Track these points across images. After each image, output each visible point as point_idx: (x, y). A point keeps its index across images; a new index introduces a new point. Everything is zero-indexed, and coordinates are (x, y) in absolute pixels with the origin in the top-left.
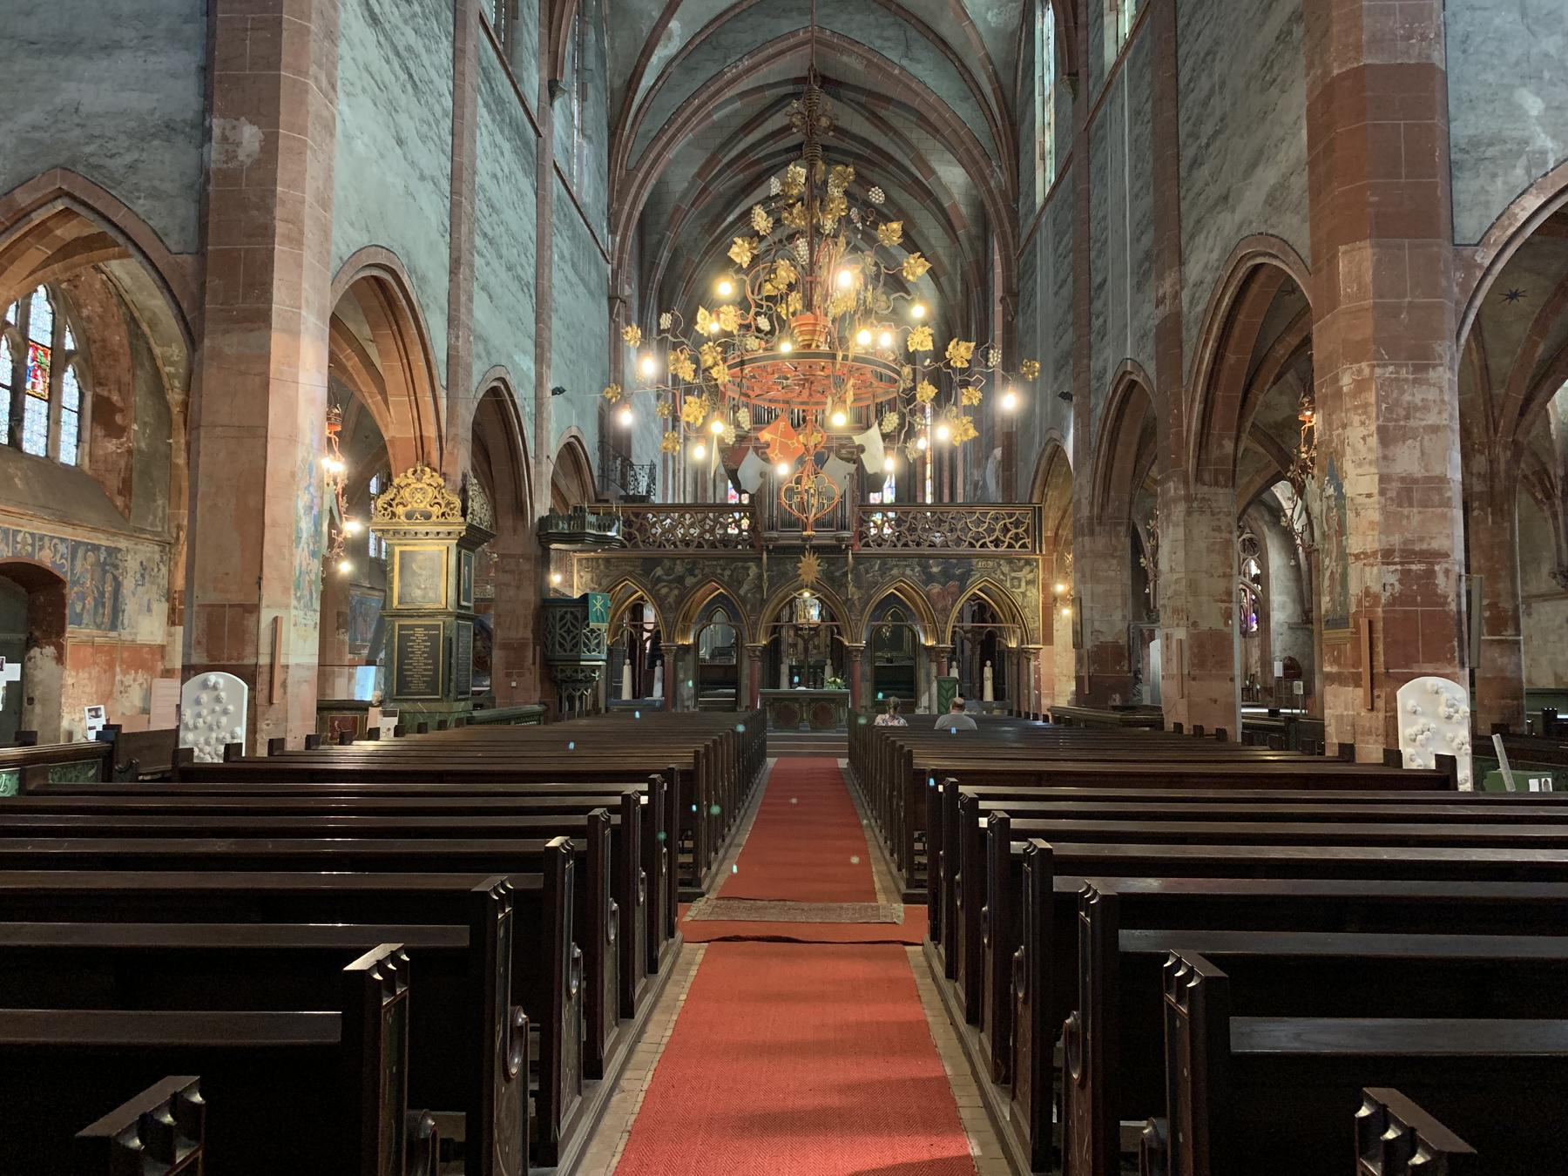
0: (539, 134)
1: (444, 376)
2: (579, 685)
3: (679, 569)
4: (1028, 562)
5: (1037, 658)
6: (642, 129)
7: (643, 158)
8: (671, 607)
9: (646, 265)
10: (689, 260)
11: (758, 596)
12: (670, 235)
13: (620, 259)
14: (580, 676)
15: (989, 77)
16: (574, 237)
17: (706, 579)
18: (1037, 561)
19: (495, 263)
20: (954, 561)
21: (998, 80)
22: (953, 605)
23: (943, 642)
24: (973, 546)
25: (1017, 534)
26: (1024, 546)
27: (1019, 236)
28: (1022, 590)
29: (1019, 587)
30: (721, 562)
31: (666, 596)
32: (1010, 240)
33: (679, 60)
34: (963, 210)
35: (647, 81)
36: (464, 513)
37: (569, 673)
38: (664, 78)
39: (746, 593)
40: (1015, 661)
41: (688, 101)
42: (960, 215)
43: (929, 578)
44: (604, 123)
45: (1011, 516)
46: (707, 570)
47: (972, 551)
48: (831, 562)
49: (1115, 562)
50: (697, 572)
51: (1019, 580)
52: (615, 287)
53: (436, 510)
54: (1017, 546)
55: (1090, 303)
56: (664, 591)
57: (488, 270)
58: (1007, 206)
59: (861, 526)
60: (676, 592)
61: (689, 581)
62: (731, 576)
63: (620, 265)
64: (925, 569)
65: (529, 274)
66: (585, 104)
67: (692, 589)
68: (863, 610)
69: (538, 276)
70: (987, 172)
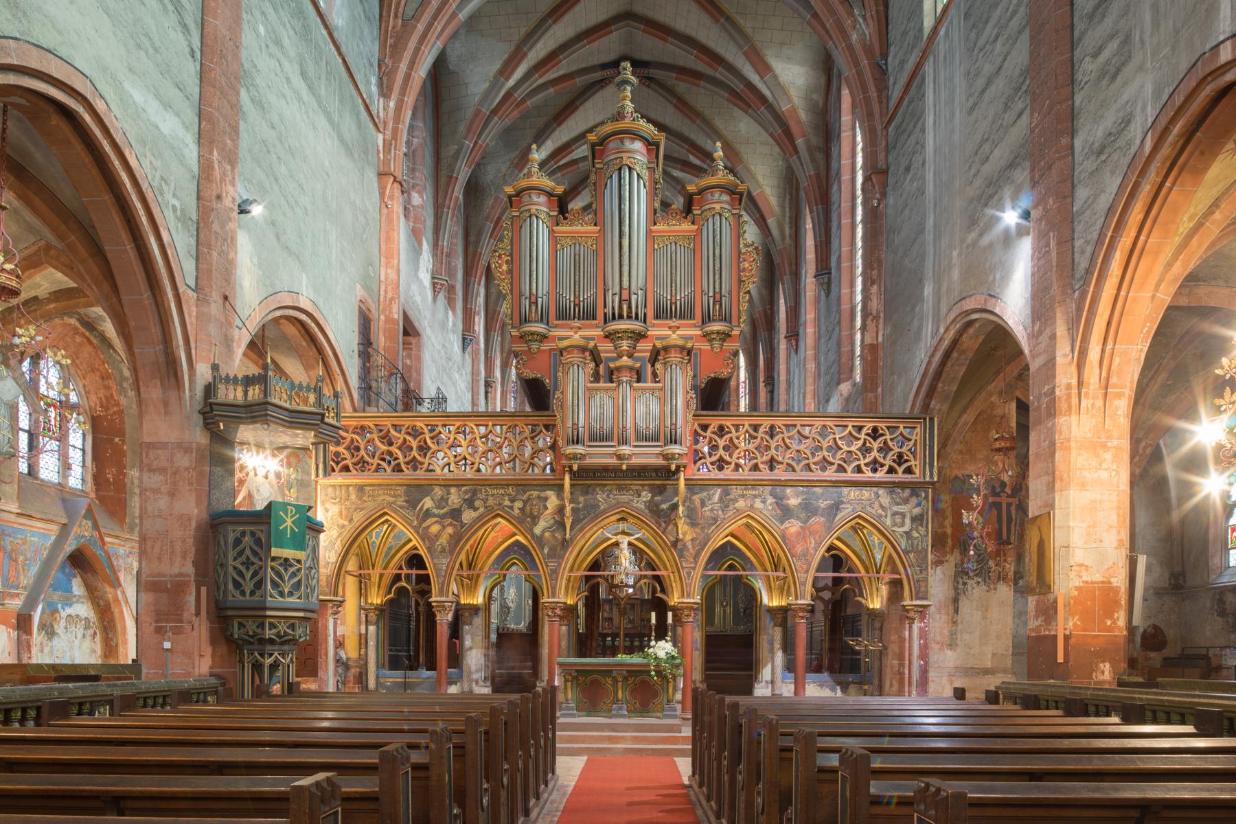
3: (455, 498)
8: (443, 550)
11: (558, 535)
17: (493, 513)
23: (804, 598)
24: (845, 471)
28: (906, 528)
29: (903, 524)
30: (510, 490)
31: (438, 536)
37: (251, 627)
39: (544, 531)
43: (786, 513)
46: (491, 502)
50: (477, 503)
51: (903, 516)
54: (900, 470)
56: (435, 529)
60: (450, 530)
61: (468, 516)
62: (522, 510)
67: (471, 526)
68: (696, 556)
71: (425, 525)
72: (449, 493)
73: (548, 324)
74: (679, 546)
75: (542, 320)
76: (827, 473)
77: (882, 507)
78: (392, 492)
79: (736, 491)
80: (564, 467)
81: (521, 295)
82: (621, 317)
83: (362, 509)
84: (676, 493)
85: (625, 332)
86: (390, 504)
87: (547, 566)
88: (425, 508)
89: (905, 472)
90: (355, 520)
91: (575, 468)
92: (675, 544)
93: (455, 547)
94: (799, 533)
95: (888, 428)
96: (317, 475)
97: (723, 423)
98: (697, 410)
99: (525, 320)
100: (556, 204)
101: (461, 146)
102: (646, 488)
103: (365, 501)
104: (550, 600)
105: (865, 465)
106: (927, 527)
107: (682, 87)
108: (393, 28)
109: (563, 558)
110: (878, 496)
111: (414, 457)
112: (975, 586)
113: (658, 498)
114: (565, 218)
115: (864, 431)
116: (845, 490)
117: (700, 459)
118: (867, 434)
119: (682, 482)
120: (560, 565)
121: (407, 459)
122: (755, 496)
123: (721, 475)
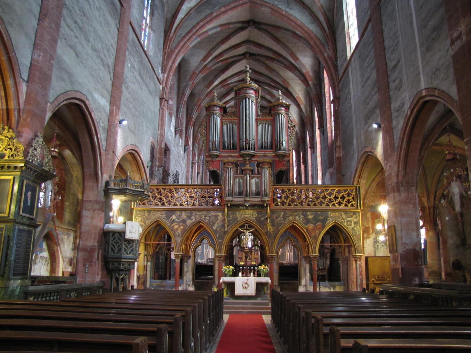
0: (122, 5)
1: (27, 74)
2: (121, 272)
4: (355, 213)
5: (360, 261)
6: (178, 34)
7: (178, 44)
8: (179, 235)
9: (180, 95)
10: (199, 98)
11: (223, 230)
12: (191, 83)
13: (166, 84)
14: (122, 267)
15: (322, 14)
16: (141, 62)
18: (358, 212)
19: (84, 42)
20: (319, 213)
21: (326, 15)
22: (319, 235)
23: (315, 253)
24: (328, 205)
25: (349, 200)
26: (352, 205)
27: (339, 74)
28: (352, 226)
29: (351, 225)
30: (205, 213)
31: (177, 229)
32: (334, 76)
33: (195, 9)
34: (311, 74)
35: (181, 16)
36: (26, 153)
38: (188, 15)
39: (217, 227)
40: (346, 262)
41: (198, 23)
42: (310, 76)
44: (162, 30)
45: (345, 191)
46: (197, 216)
47: (327, 208)
48: (259, 213)
49: (411, 206)
50: (192, 217)
51: (351, 222)
52: (163, 94)
53: (7, 153)
55: (388, 78)
56: (176, 227)
57: (76, 40)
58: (333, 64)
59: (274, 195)
60: (182, 227)
63: (166, 86)
64: (305, 216)
65: (111, 61)
66: (153, 18)
67: (190, 225)
68: (275, 238)
69: (115, 65)
70: (323, 50)
71: (172, 225)
72: (182, 214)
73: (219, 151)
74: (268, 234)
75: (217, 150)
76: (322, 206)
77: (343, 219)
78: (161, 213)
79: (289, 213)
80: (225, 205)
81: (209, 141)
82: (246, 149)
83: (149, 219)
84: (267, 214)
85: (247, 154)
86: (160, 217)
87: (218, 241)
88: (173, 219)
89: (350, 206)
90: (147, 223)
91: (229, 205)
92: (266, 233)
93: (184, 234)
94: (312, 229)
95: (344, 190)
96: (134, 206)
97: (284, 188)
98: (274, 183)
99: (210, 150)
100: (222, 110)
101: (188, 83)
102: (255, 212)
103: (151, 216)
104: (219, 254)
105: (337, 203)
106: (360, 226)
107: (268, 62)
108: (168, 51)
109: (224, 238)
110: (341, 214)
111: (170, 200)
112: (381, 246)
113: (259, 216)
114: (226, 115)
115: (335, 191)
116: (329, 213)
117: (275, 201)
118: (336, 192)
119: (269, 210)
120: (223, 241)
121: (167, 201)
122: (296, 215)
123: (283, 208)
